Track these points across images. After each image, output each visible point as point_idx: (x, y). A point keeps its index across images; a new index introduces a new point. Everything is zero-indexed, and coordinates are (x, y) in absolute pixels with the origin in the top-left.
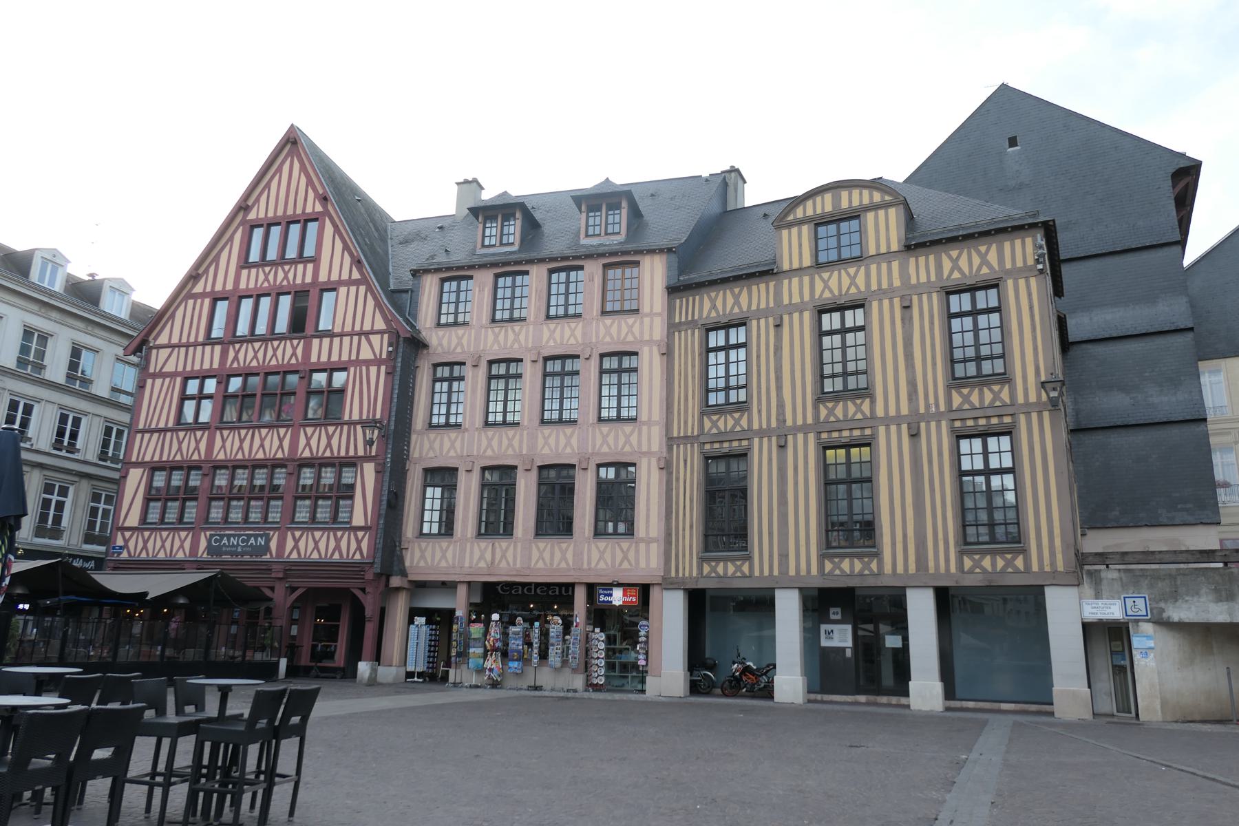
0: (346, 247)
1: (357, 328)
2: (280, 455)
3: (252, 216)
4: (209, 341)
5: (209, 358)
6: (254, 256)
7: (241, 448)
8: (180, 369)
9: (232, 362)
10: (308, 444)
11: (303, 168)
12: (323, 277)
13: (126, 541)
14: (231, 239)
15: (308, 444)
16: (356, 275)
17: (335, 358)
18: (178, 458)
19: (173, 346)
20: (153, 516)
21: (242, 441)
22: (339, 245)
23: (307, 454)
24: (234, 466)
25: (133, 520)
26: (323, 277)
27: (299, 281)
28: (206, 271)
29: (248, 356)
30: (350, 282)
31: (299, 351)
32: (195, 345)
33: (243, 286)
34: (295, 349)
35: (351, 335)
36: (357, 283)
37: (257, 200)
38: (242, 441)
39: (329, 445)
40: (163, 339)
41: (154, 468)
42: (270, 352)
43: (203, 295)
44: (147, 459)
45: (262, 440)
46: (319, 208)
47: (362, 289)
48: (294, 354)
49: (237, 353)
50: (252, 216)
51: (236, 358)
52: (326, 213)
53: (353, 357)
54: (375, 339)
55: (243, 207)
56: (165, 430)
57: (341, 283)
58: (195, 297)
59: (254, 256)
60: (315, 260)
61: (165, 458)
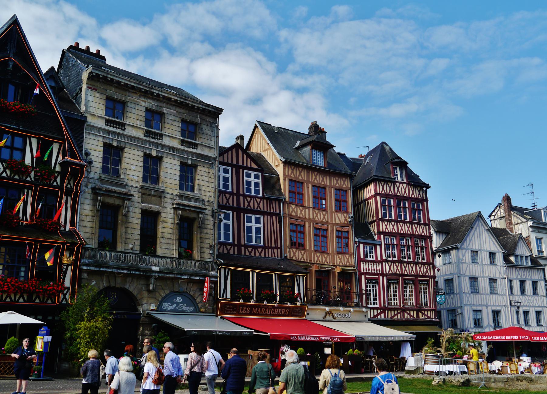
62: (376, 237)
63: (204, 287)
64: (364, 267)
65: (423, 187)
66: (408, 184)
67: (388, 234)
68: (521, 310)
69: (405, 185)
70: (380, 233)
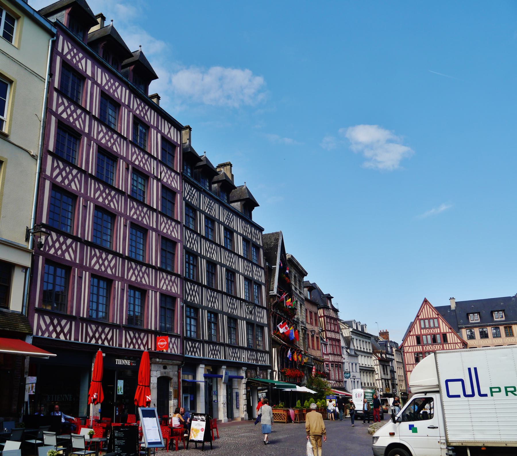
0: (446, 325)
3: (420, 317)
6: (423, 326)
11: (430, 307)
12: (442, 331)
14: (416, 323)
16: (450, 331)
26: (442, 331)
30: (449, 332)
31: (441, 347)
32: (415, 346)
33: (423, 333)
35: (453, 343)
40: (406, 345)
43: (413, 335)
52: (439, 317)
54: (459, 344)
55: (418, 316)
57: (447, 332)
58: (411, 335)
59: (423, 326)
60: (439, 327)
62: (325, 340)
63: (312, 371)
64: (325, 357)
65: (336, 311)
66: (333, 310)
67: (331, 339)
68: (356, 380)
70: (327, 338)
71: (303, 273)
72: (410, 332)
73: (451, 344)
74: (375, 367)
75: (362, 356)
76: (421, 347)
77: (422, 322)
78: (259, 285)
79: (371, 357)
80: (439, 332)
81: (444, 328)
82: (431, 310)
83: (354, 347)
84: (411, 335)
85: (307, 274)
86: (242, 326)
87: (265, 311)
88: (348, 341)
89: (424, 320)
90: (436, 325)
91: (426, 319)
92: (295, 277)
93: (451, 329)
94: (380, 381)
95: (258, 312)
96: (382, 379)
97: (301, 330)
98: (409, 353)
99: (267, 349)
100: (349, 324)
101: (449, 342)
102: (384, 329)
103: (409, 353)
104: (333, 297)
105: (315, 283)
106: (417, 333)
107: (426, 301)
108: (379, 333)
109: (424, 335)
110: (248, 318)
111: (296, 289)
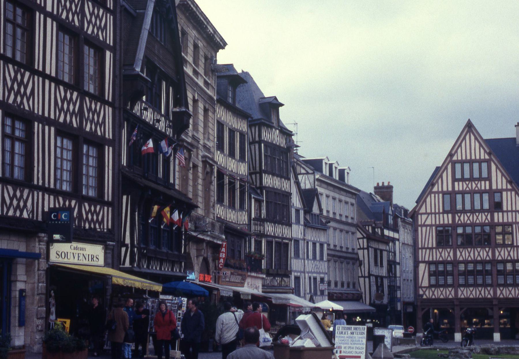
0: (503, 175)
1: (514, 209)
2: (488, 258)
3: (455, 158)
4: (445, 212)
5: (447, 219)
6: (458, 176)
7: (469, 256)
8: (434, 223)
9: (458, 221)
10: (500, 254)
11: (476, 138)
12: (494, 187)
13: (424, 292)
14: (446, 168)
15: (500, 254)
16: (509, 187)
17: (505, 220)
18: (441, 259)
19: (429, 214)
20: (433, 282)
21: (469, 253)
22: (499, 175)
23: (500, 258)
24: (466, 262)
25: (425, 283)
27: (483, 188)
28: (437, 182)
29: (464, 218)
30: (507, 190)
32: (439, 213)
33: (456, 189)
34: (486, 216)
35: (512, 211)
36: (511, 190)
37: (456, 152)
38: (469, 253)
39: (509, 255)
40: (423, 210)
41: (429, 263)
42: (475, 218)
43: (438, 192)
44: (427, 259)
45: (479, 253)
46: (487, 157)
47: (513, 193)
48: (486, 218)
49: (459, 217)
50: (455, 158)
51: (459, 219)
53: (514, 221)
55: (451, 155)
56: (431, 249)
58: (435, 193)
59: (458, 176)
60: (489, 179)
61: (435, 259)
65: (287, 134)
69: (278, 131)
71: (216, 43)
72: (433, 185)
73: (507, 211)
74: (360, 252)
75: (335, 229)
76: (450, 216)
77: (458, 166)
78: (100, 49)
79: (353, 233)
80: (488, 188)
81: (499, 180)
82: (477, 145)
83: (321, 210)
84: (435, 193)
85: (225, 44)
86: (45, 137)
87: (109, 111)
88: (309, 197)
89: (462, 162)
90: (485, 175)
91: (466, 161)
92: (196, 46)
93: (510, 182)
94: (367, 280)
95: (90, 110)
96: (370, 275)
97: (200, 165)
98: (426, 226)
99: (108, 195)
100: (316, 165)
101: (505, 209)
102: (383, 180)
103: (426, 226)
104: (282, 105)
105: (247, 74)
106: (445, 189)
107: (469, 127)
108: (375, 188)
109: (459, 192)
110: (61, 120)
111: (196, 73)
